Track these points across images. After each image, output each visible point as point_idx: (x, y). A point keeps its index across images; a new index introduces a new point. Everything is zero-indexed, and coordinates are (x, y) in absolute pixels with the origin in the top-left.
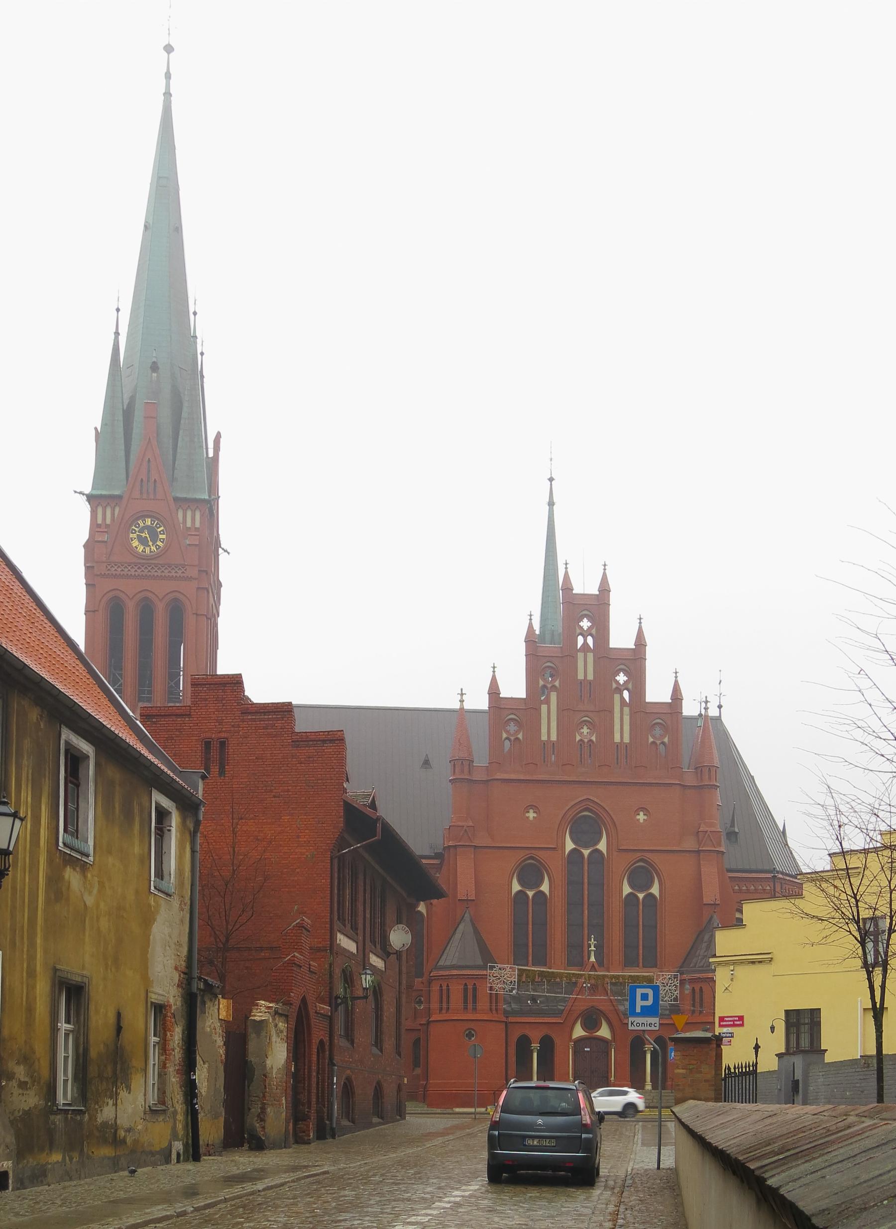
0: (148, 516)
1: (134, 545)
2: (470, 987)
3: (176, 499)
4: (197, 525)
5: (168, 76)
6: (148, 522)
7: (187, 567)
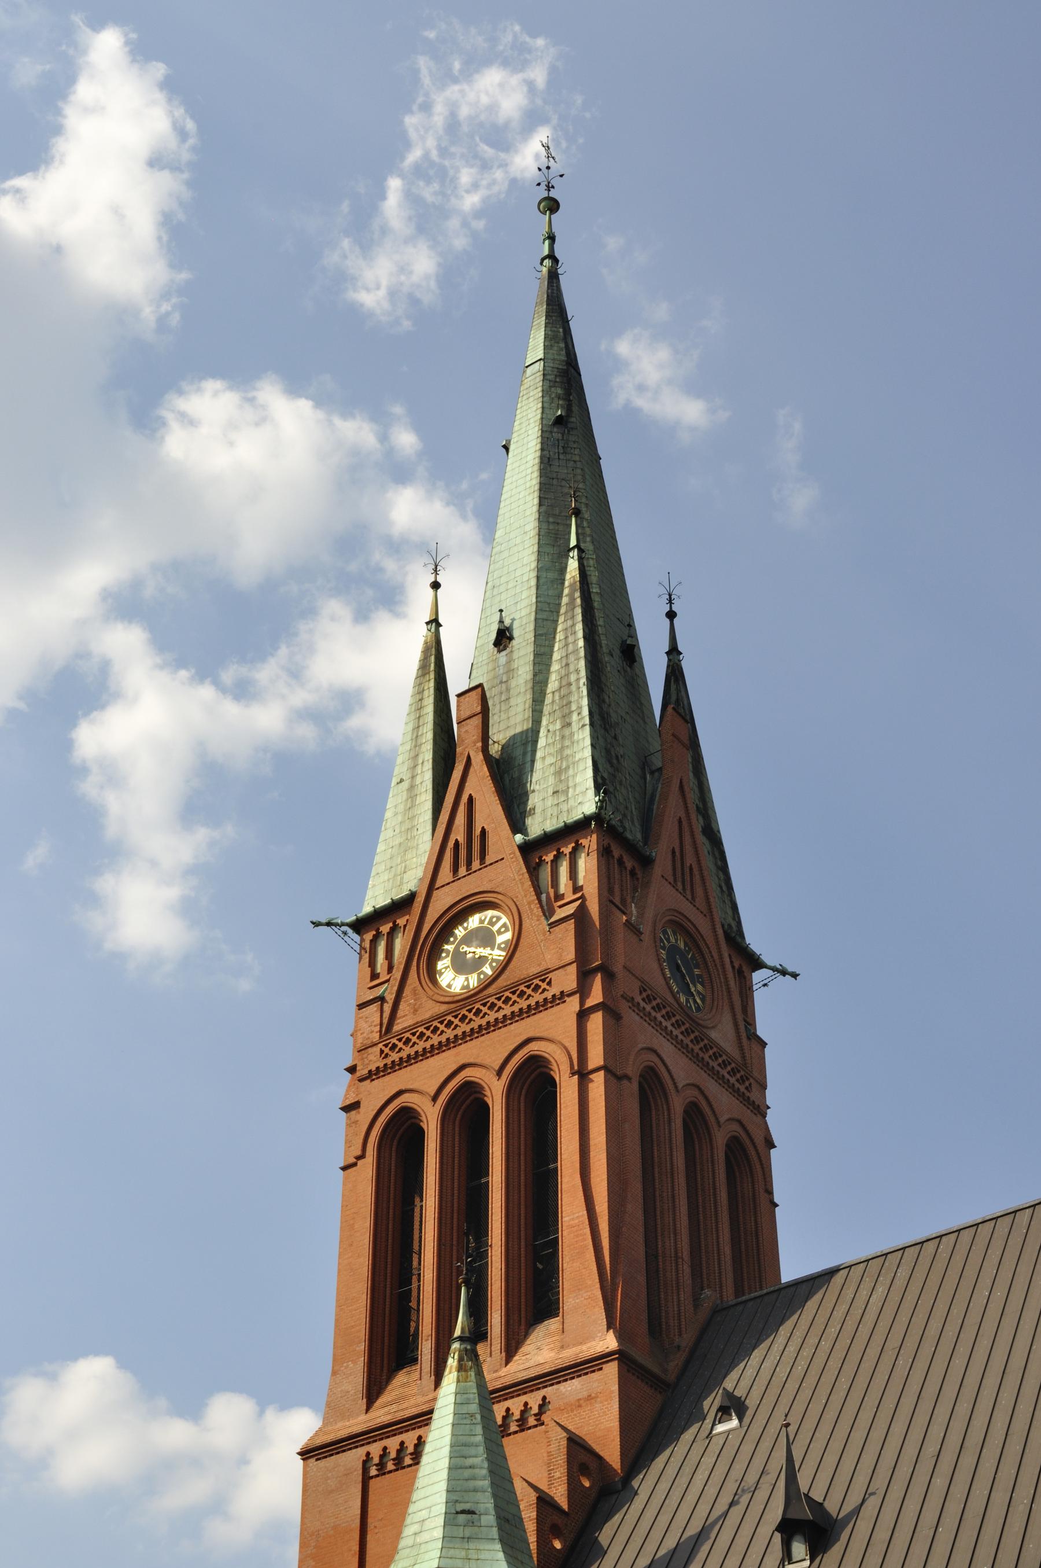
7: (550, 975)
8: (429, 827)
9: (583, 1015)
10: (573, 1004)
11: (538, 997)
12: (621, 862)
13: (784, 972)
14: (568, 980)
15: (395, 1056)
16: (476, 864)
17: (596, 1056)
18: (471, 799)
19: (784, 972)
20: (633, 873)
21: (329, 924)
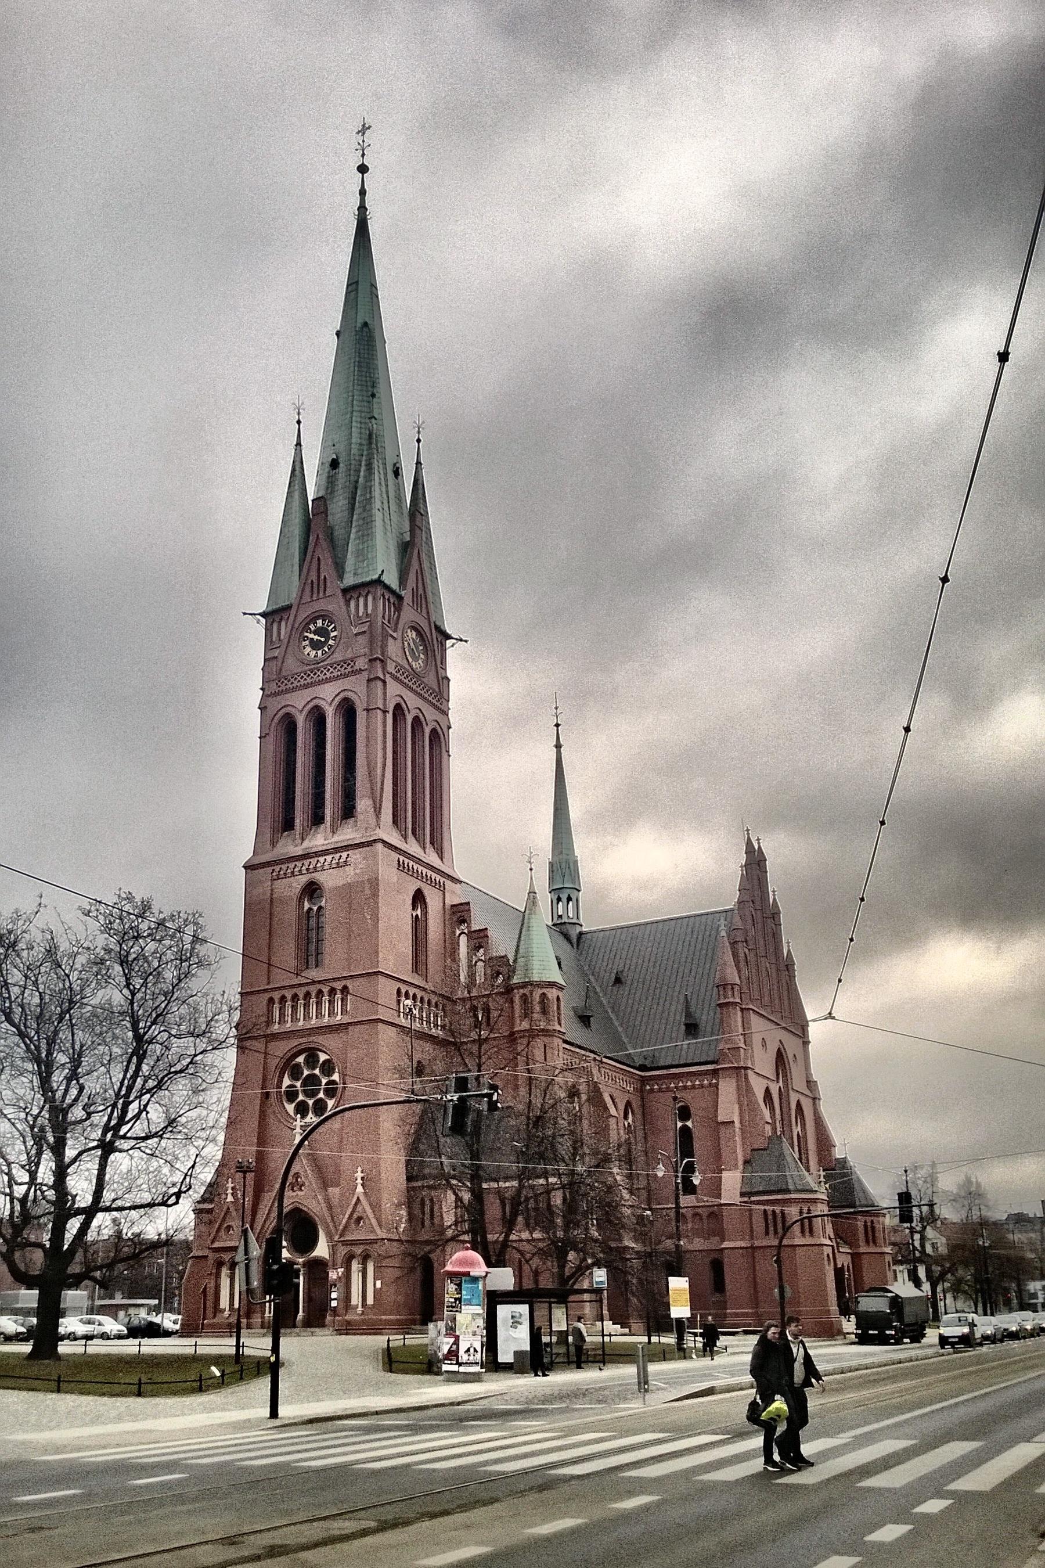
0: (318, 618)
1: (306, 653)
3: (345, 591)
4: (369, 612)
5: (363, 193)
6: (320, 623)
9: (369, 680)
10: (365, 675)
12: (389, 600)
15: (283, 687)
16: (321, 595)
19: (461, 640)
20: (394, 604)
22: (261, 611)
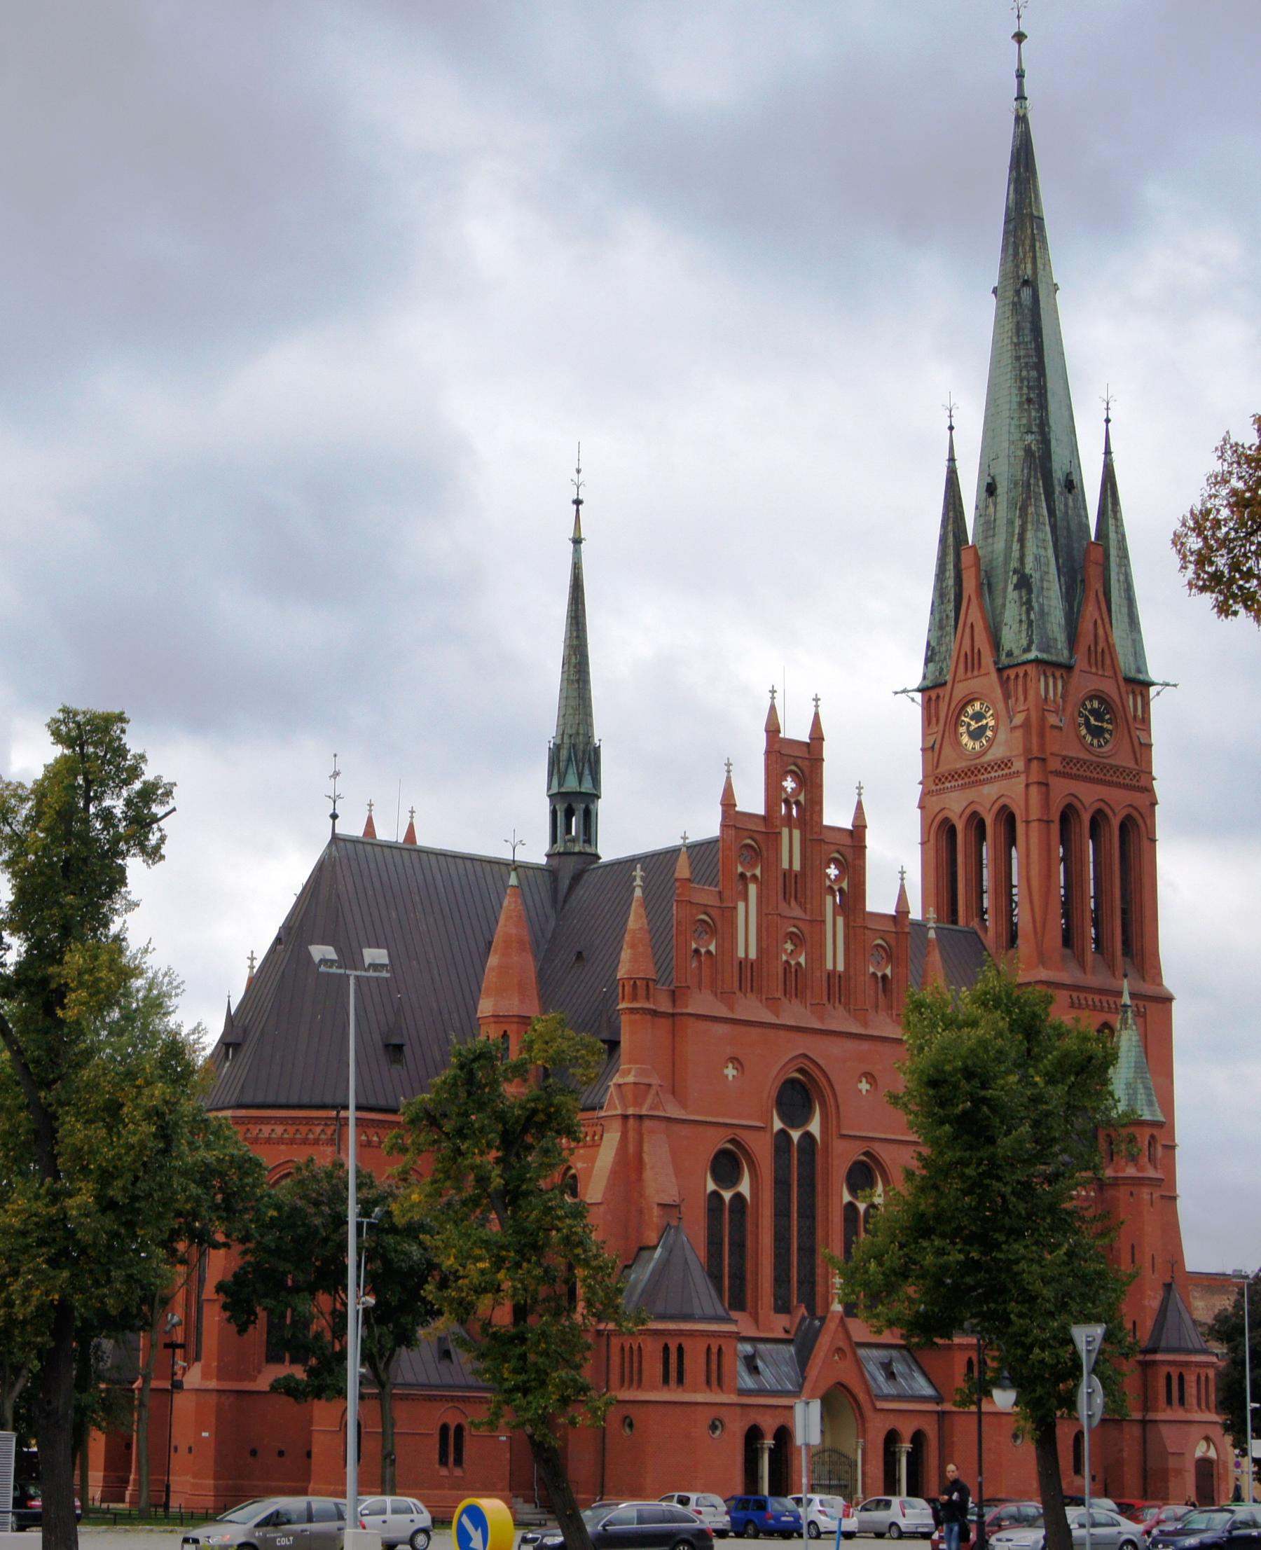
2: (714, 1350)
8: (952, 631)
9: (1027, 786)
11: (1006, 771)
13: (1167, 685)
14: (1019, 765)
17: (1035, 814)
18: (972, 625)
19: (1167, 685)
21: (904, 691)
22: (915, 687)
